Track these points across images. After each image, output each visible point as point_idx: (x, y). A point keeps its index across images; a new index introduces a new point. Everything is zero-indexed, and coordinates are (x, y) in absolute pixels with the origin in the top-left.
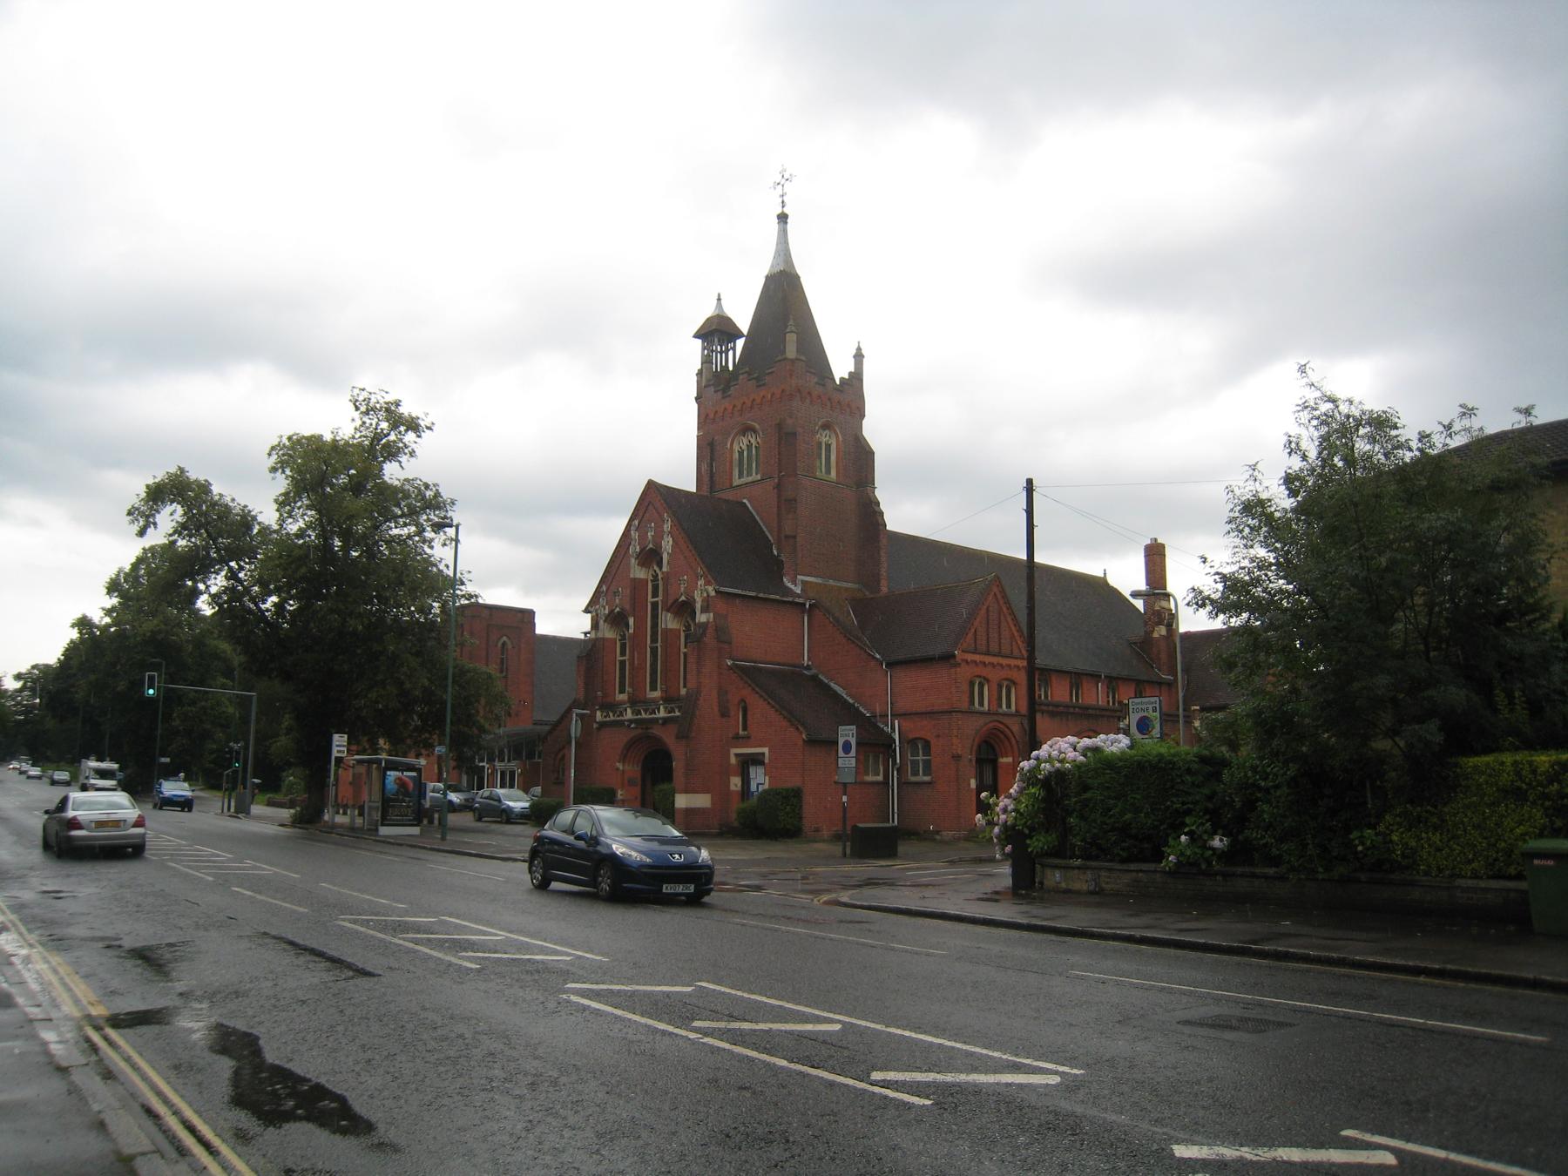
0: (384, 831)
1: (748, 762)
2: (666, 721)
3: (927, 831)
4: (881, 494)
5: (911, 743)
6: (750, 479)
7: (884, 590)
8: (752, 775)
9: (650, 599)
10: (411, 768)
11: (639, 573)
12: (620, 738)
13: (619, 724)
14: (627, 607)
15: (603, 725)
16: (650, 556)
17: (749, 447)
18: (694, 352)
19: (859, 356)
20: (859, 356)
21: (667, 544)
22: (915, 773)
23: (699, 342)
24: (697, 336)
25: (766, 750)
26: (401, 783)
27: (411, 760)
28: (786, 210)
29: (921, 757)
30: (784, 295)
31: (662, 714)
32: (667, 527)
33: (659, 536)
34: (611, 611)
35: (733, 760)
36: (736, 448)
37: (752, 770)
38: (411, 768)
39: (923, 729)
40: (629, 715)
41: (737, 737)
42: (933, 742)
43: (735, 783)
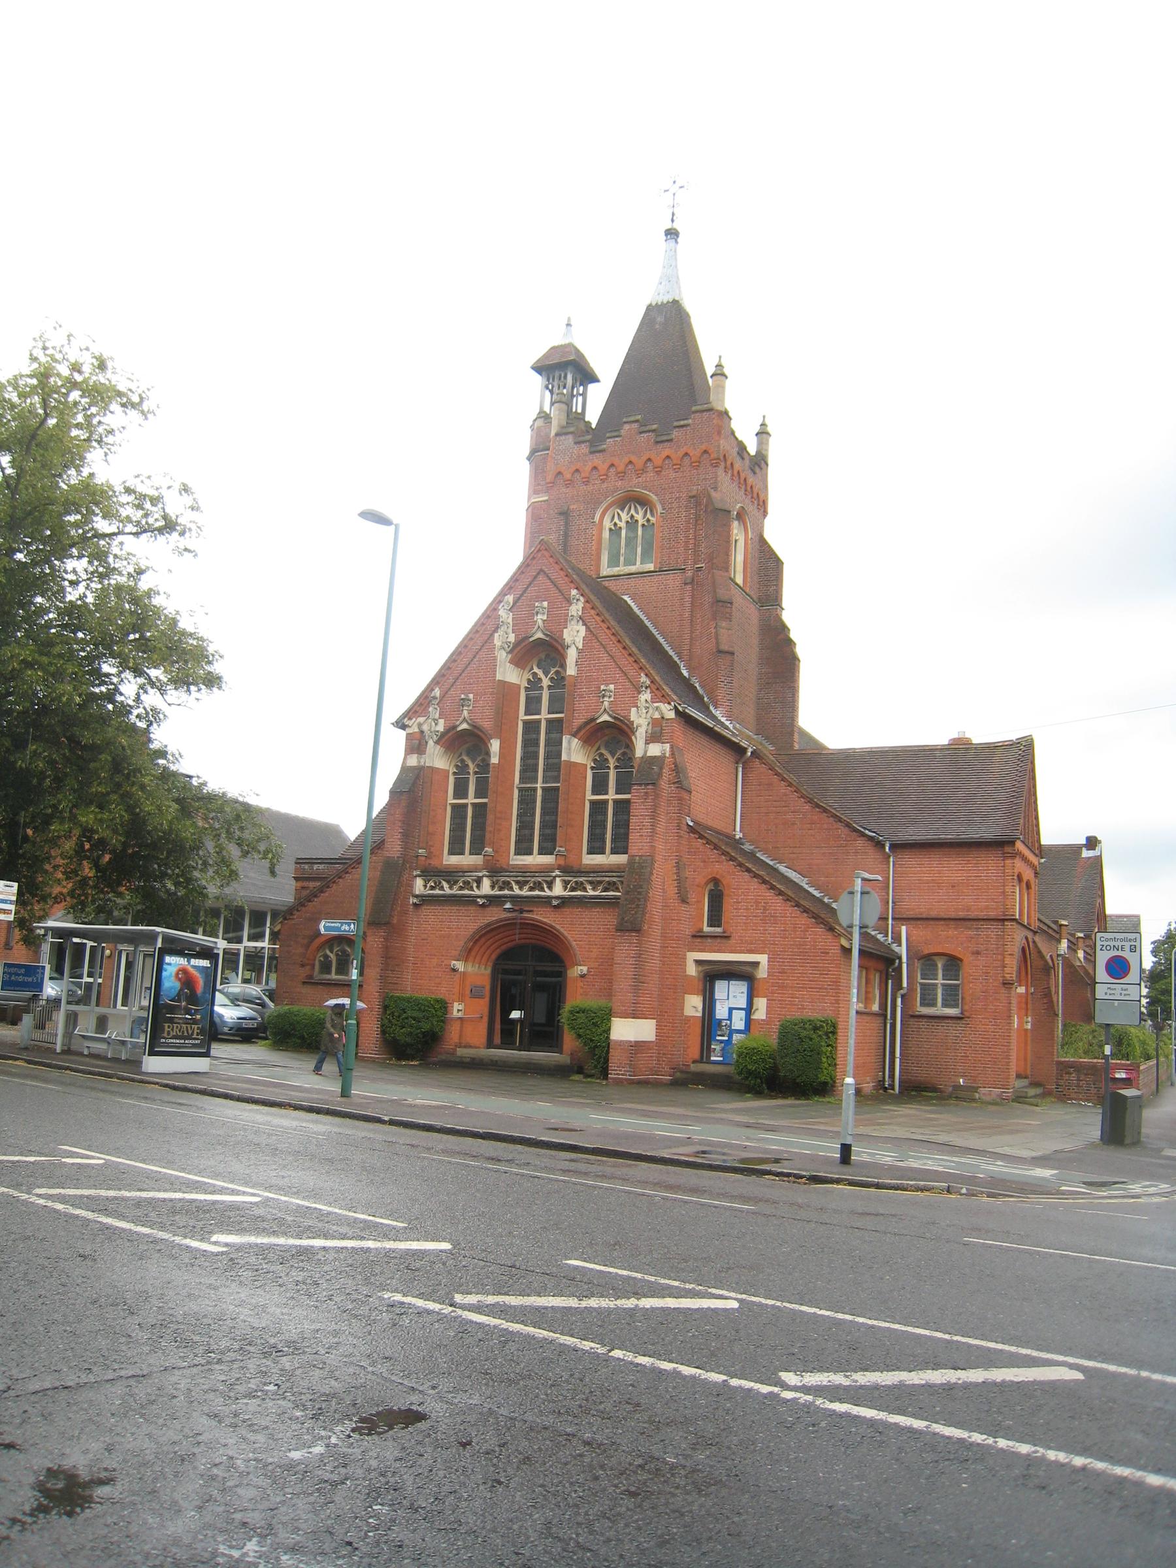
0: (154, 1064)
1: (714, 974)
2: (564, 902)
3: (957, 1087)
4: (787, 617)
5: (926, 960)
6: (633, 569)
7: (797, 747)
8: (717, 995)
9: (522, 716)
10: (207, 953)
11: (510, 674)
12: (468, 923)
13: (471, 901)
14: (487, 724)
15: (425, 900)
16: (543, 651)
17: (632, 524)
18: (533, 395)
19: (763, 433)
20: (763, 433)
21: (574, 635)
22: (929, 1001)
23: (538, 380)
24: (539, 368)
25: (763, 959)
26: (186, 979)
27: (200, 938)
28: (675, 225)
29: (940, 981)
30: (666, 341)
31: (558, 890)
32: (576, 609)
33: (559, 620)
34: (451, 729)
35: (692, 970)
36: (607, 524)
37: (721, 988)
38: (207, 953)
39: (950, 940)
40: (486, 888)
41: (699, 936)
42: (968, 959)
43: (693, 1005)
